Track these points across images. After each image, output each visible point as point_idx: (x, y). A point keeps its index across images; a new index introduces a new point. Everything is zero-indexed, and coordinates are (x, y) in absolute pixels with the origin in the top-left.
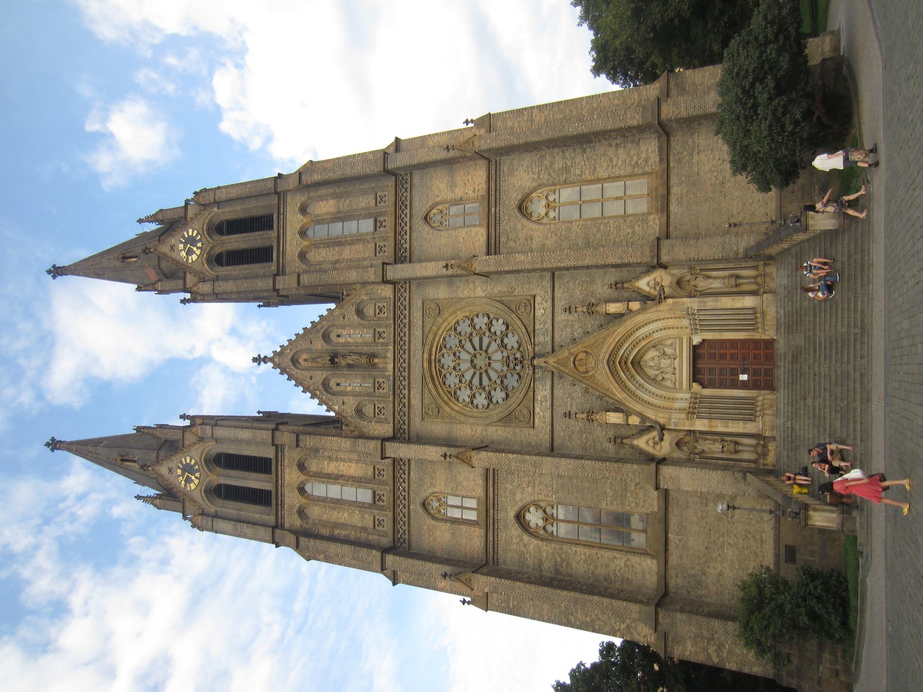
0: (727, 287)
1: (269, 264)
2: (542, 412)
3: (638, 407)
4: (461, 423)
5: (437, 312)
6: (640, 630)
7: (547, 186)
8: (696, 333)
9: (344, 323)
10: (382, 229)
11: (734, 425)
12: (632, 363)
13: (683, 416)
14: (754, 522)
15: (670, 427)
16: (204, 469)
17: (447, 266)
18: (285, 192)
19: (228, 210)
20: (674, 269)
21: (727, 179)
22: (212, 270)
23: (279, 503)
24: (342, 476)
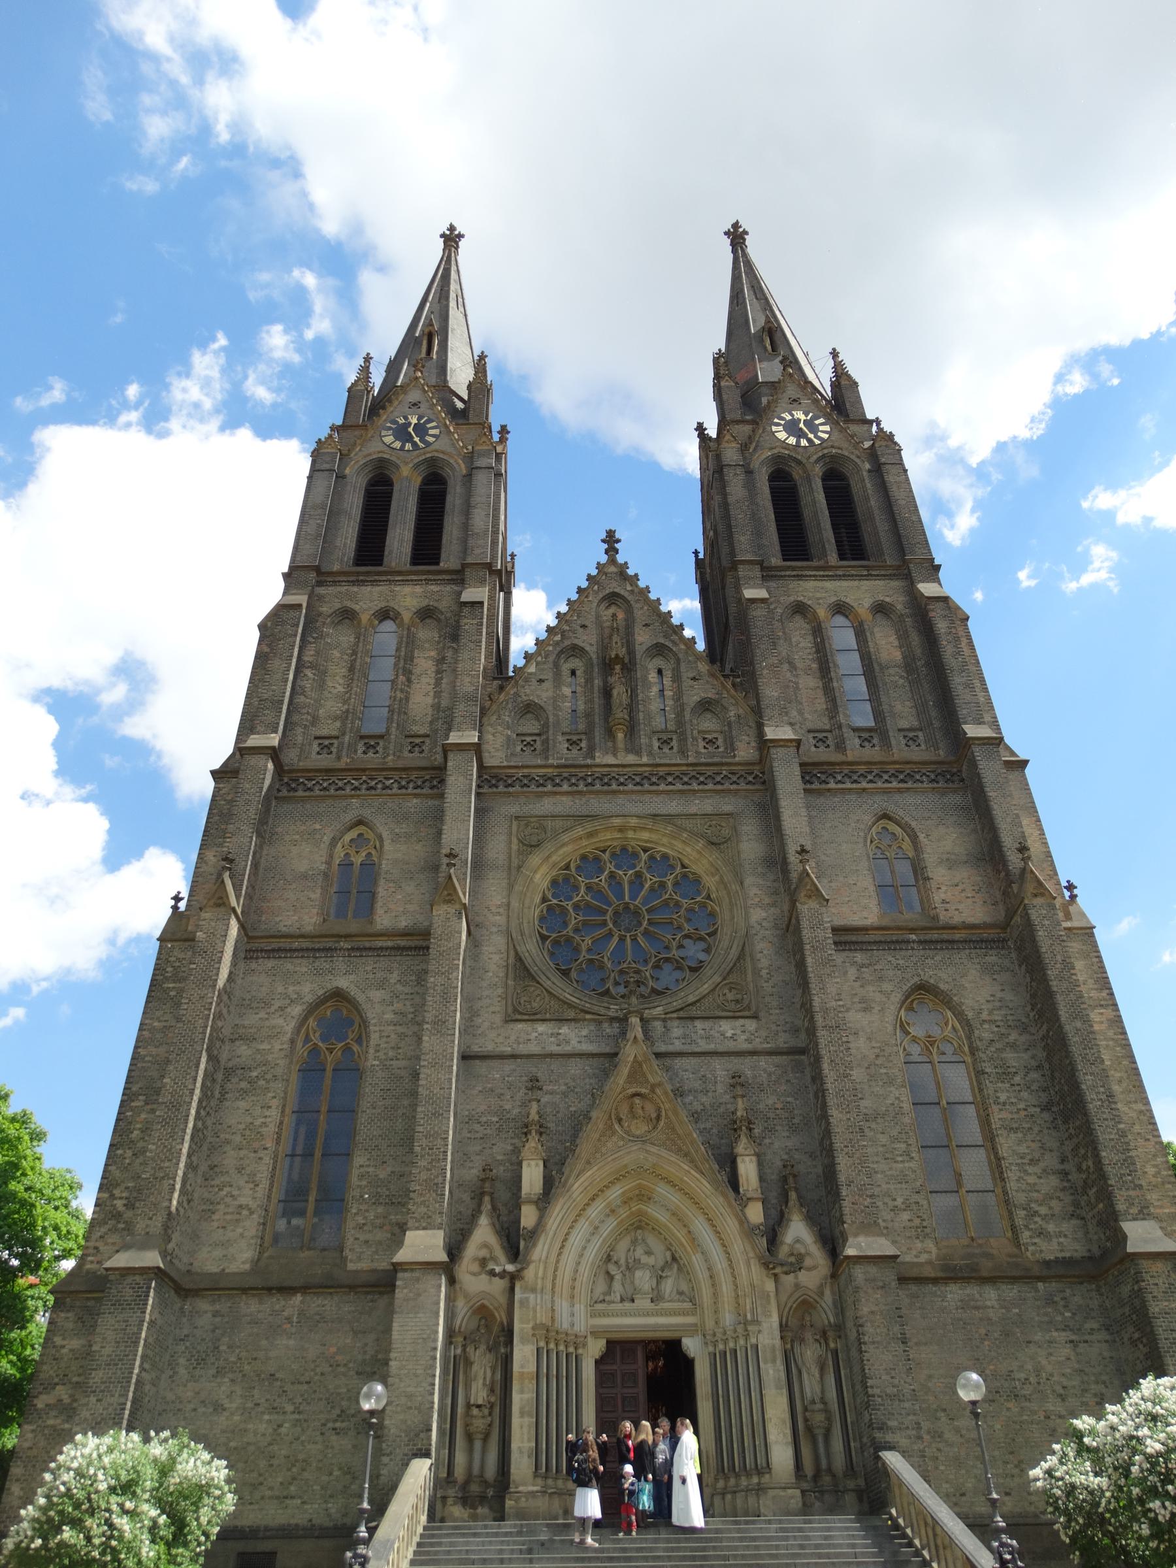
0: (806, 1409)
1: (779, 555)
4: (511, 887)
5: (714, 840)
6: (110, 1241)
7: (969, 1038)
8: (706, 1343)
9: (684, 678)
10: (857, 741)
11: (525, 1430)
12: (641, 1213)
13: (542, 1317)
14: (325, 1478)
15: (517, 1289)
16: (418, 456)
17: (803, 851)
19: (869, 485)
20: (833, 1293)
21: (1027, 1404)
22: (762, 463)
24: (409, 680)
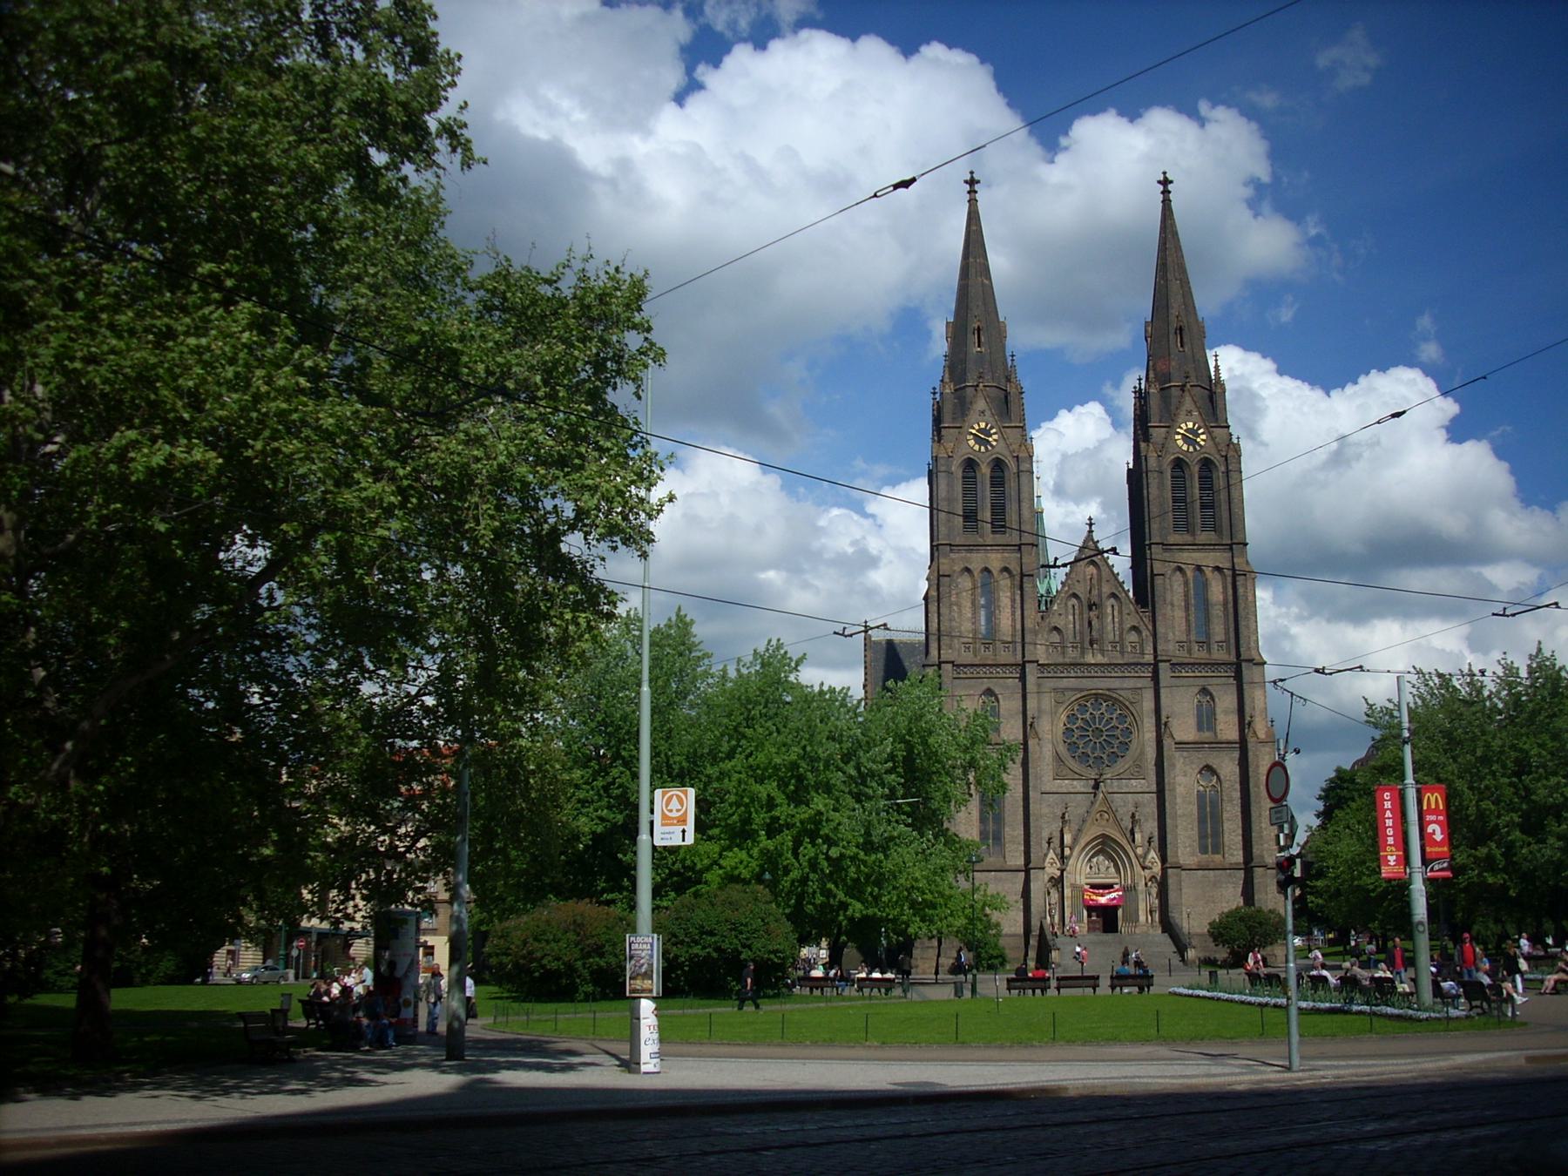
2: (1065, 785)
3: (1075, 853)
18: (1231, 549)
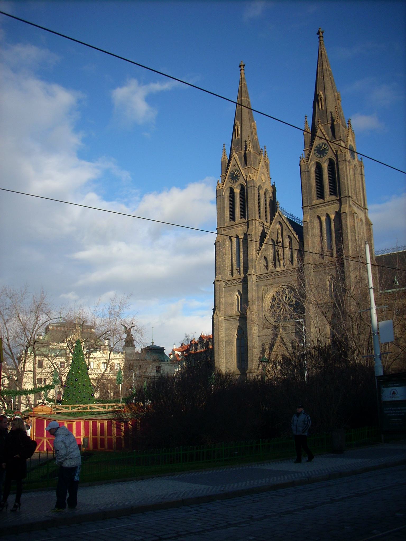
23: (231, 227)
